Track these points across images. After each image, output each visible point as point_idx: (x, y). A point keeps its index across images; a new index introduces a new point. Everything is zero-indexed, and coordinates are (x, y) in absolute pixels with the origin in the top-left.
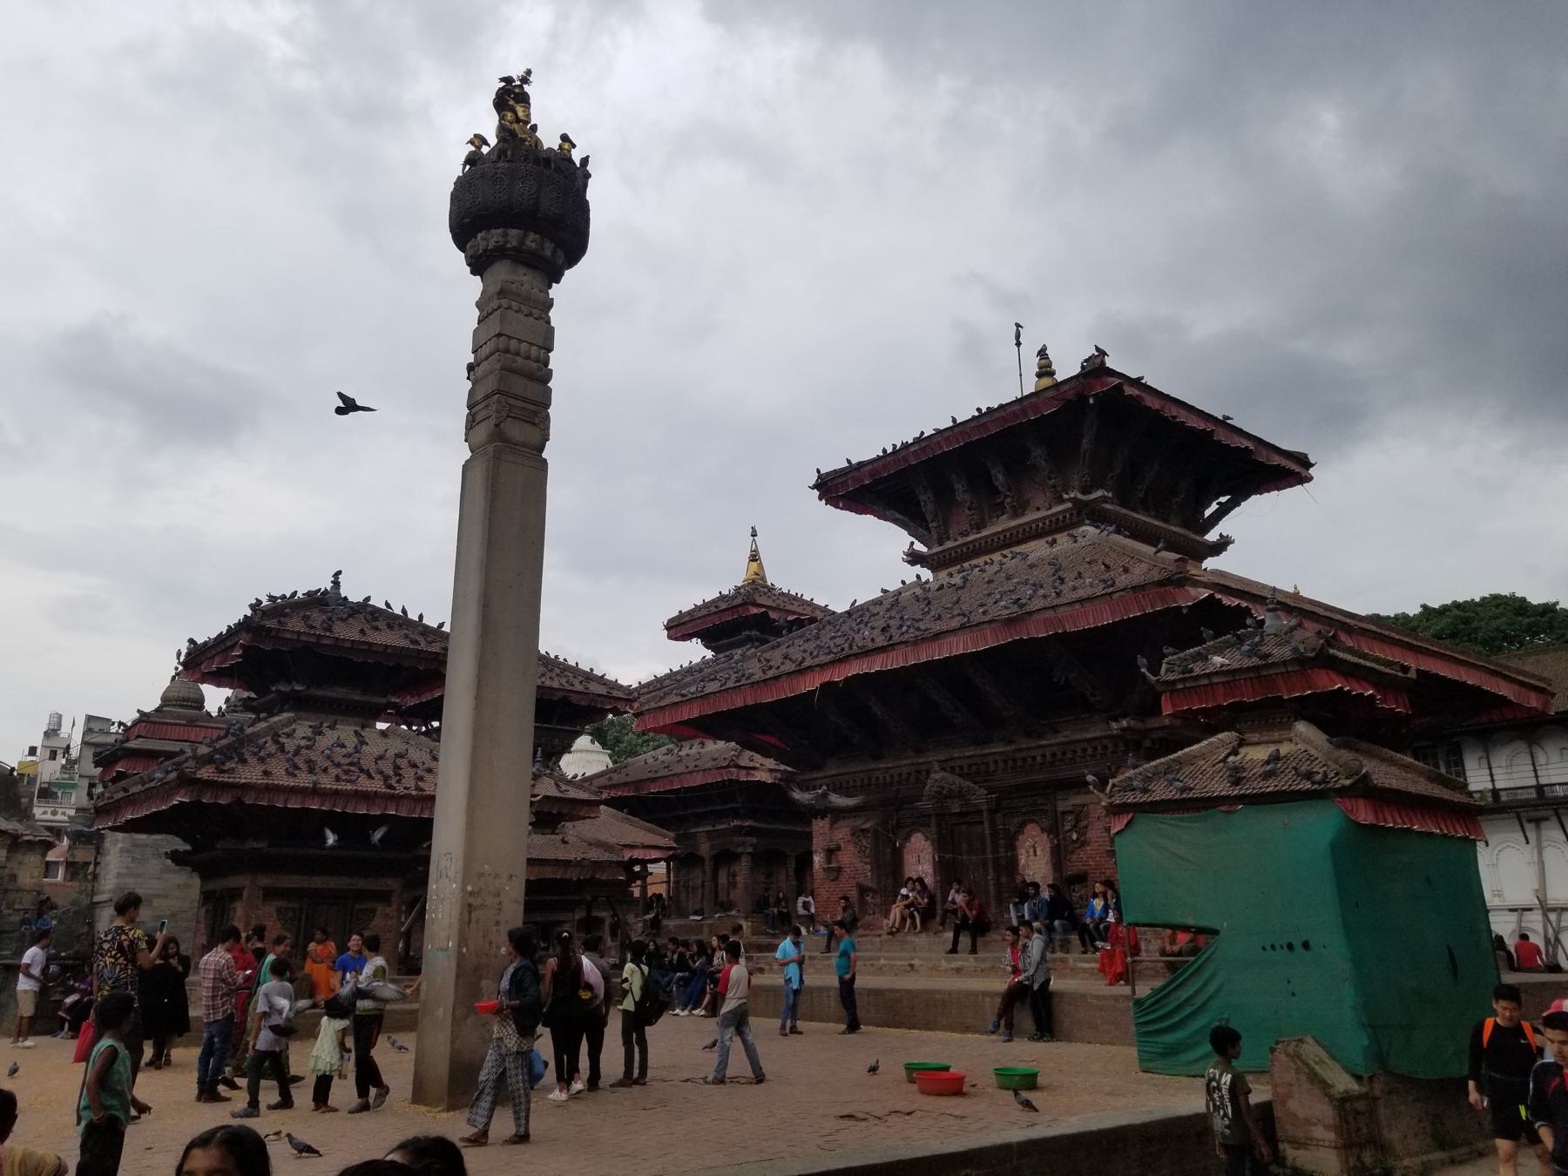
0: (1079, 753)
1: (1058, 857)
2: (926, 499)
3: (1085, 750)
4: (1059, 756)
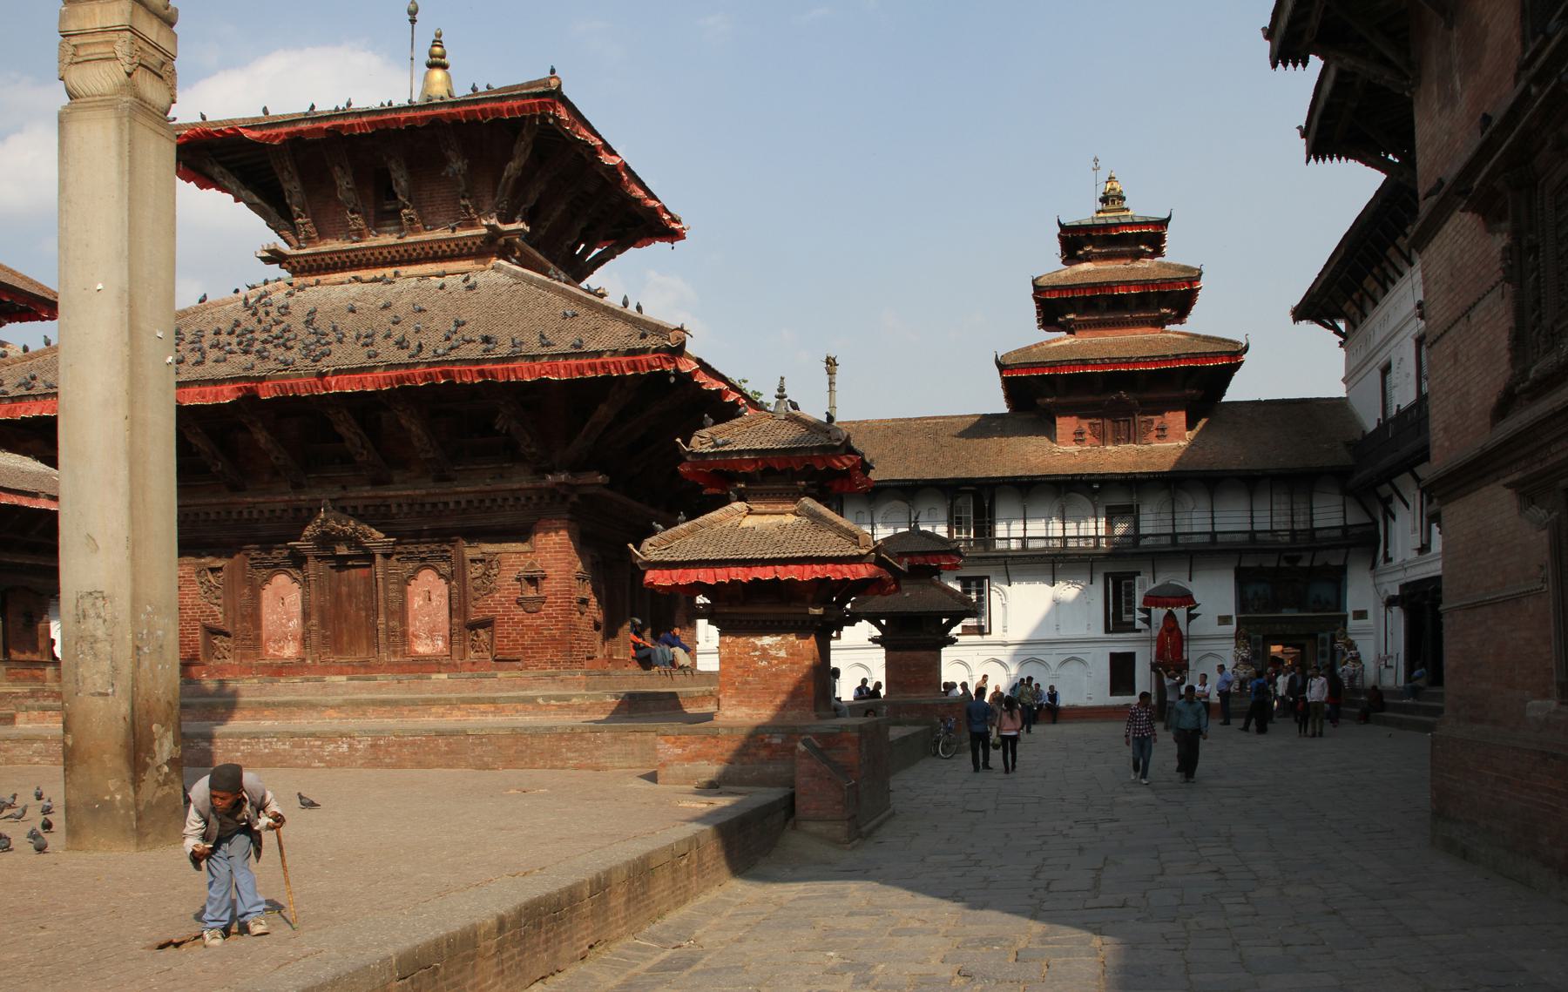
0: (499, 501)
1: (457, 607)
2: (292, 188)
3: (505, 499)
4: (476, 504)
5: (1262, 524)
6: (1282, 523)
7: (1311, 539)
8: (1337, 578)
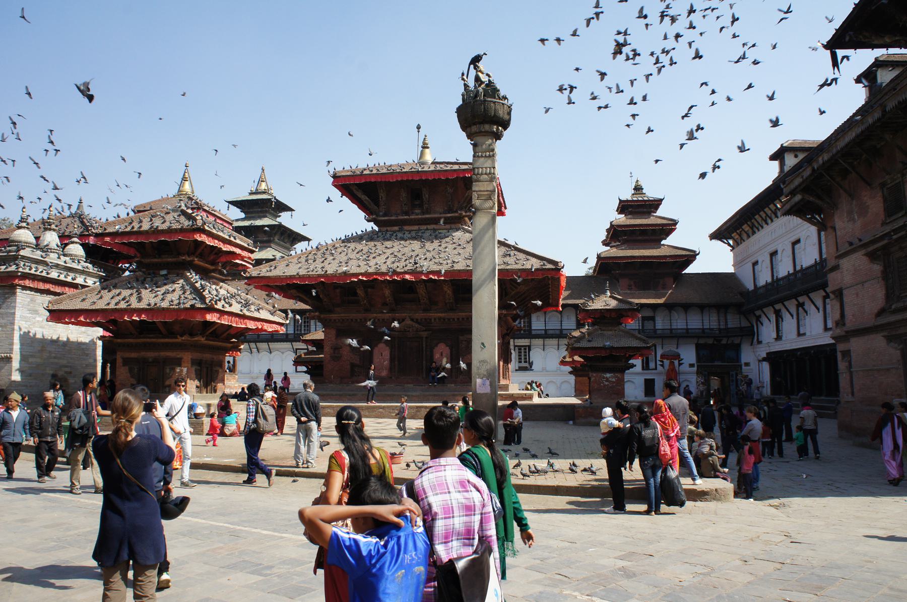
5: (707, 326)
6: (714, 325)
7: (727, 332)
8: (737, 348)
